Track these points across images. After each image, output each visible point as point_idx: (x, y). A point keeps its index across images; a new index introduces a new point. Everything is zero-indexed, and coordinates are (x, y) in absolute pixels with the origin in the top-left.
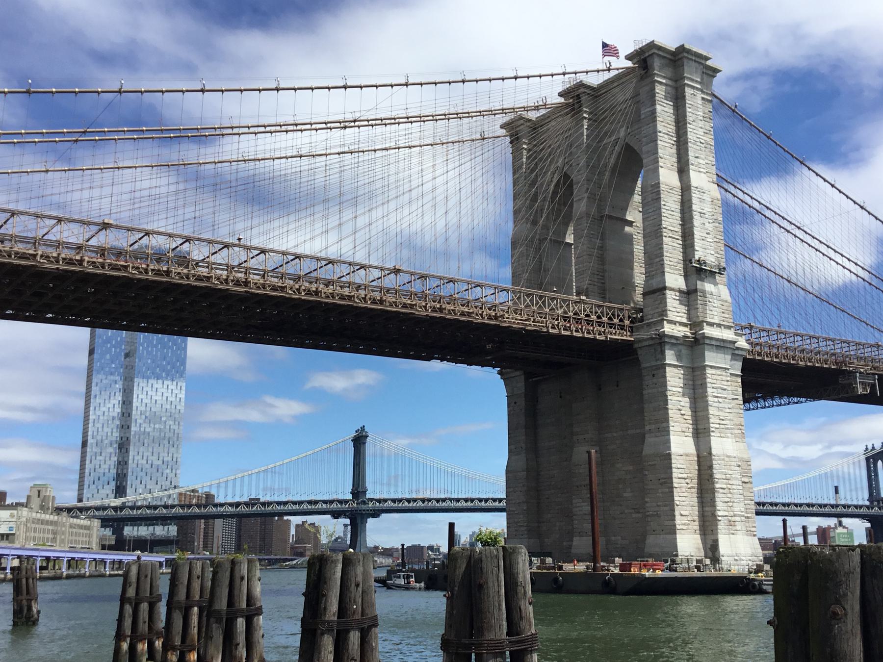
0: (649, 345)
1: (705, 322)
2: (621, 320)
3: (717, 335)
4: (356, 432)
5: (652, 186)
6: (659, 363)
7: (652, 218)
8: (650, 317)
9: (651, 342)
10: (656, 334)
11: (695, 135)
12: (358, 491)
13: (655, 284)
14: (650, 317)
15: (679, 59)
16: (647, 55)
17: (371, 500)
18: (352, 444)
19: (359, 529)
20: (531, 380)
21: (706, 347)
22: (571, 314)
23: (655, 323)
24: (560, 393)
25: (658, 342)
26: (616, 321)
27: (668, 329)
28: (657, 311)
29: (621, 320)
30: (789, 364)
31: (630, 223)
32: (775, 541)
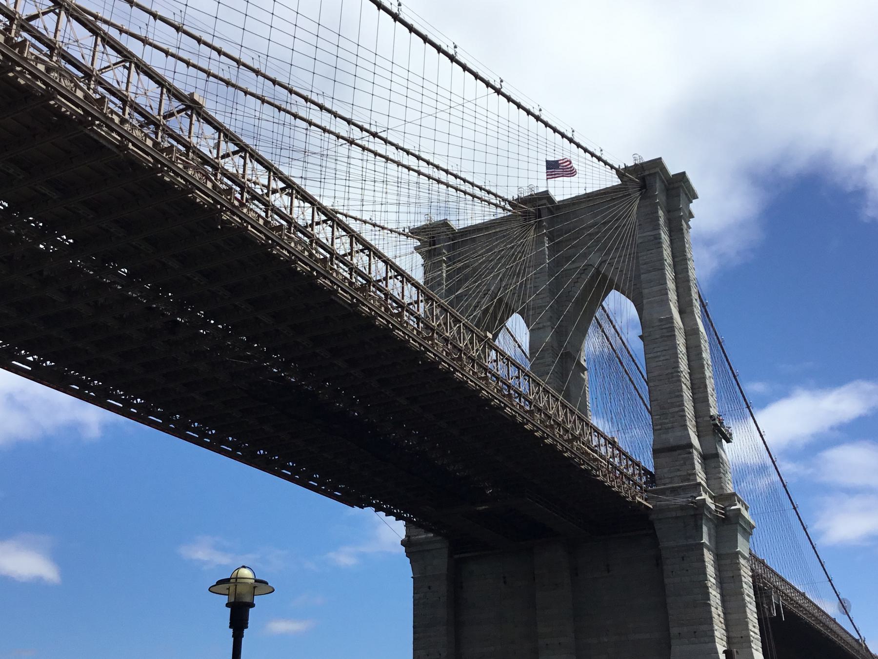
0: (677, 518)
1: (737, 496)
5: (661, 320)
6: (691, 542)
7: (662, 358)
8: (667, 481)
9: (679, 514)
10: (692, 502)
13: (672, 439)
14: (667, 481)
15: (678, 188)
16: (647, 173)
20: (456, 556)
23: (684, 489)
24: (504, 578)
25: (692, 513)
28: (678, 473)
31: (584, 369)
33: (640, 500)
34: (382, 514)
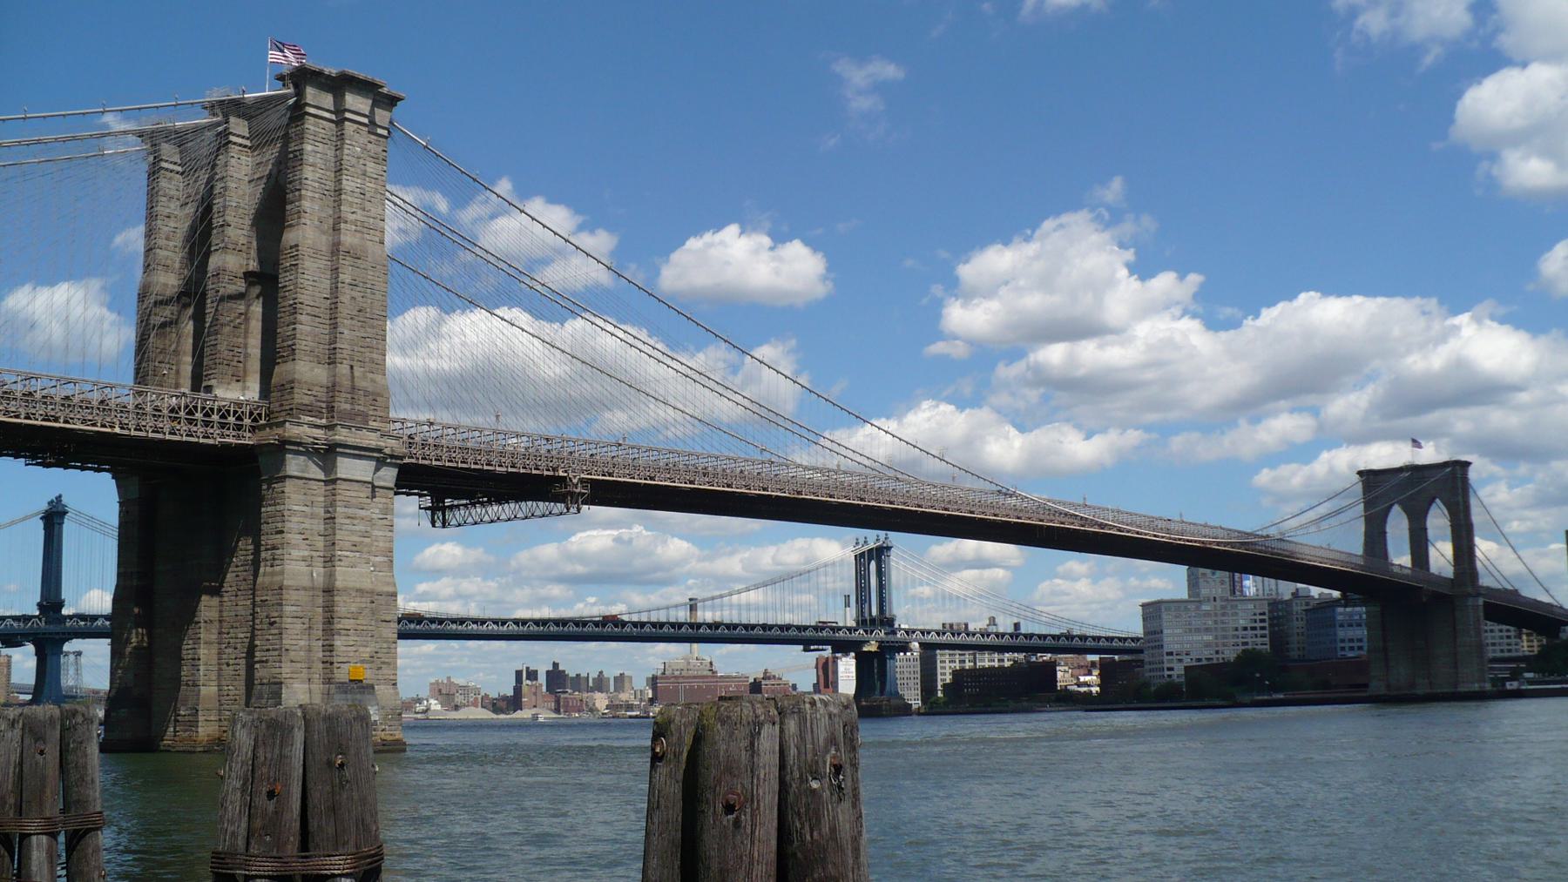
2: (239, 418)
3: (355, 442)
4: (49, 503)
5: (291, 248)
11: (353, 184)
12: (51, 603)
17: (70, 617)
18: (41, 524)
19: (48, 658)
21: (339, 459)
22: (165, 412)
26: (231, 419)
27: (292, 431)
29: (239, 418)
30: (482, 470)
32: (755, 679)
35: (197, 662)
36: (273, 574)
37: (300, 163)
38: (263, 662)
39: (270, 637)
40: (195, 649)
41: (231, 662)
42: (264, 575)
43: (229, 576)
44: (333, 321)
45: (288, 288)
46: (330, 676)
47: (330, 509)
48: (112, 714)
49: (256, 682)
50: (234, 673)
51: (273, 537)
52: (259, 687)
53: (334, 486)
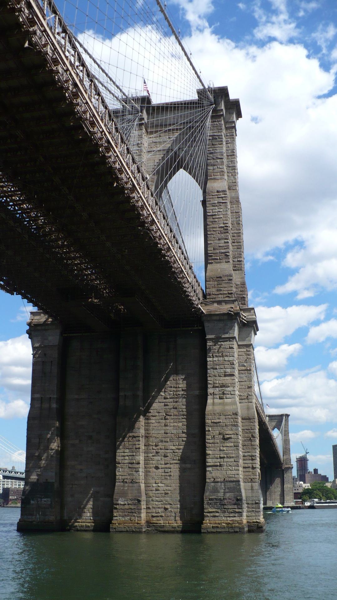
33: (200, 307)
34: (26, 300)
35: (137, 466)
36: (223, 404)
37: (221, 143)
38: (217, 466)
39: (225, 448)
40: (134, 456)
41: (160, 466)
42: (213, 404)
43: (155, 405)
44: (236, 244)
45: (218, 217)
46: (252, 477)
47: (245, 364)
48: (32, 502)
49: (207, 480)
50: (163, 474)
51: (221, 378)
52: (212, 484)
53: (248, 349)
